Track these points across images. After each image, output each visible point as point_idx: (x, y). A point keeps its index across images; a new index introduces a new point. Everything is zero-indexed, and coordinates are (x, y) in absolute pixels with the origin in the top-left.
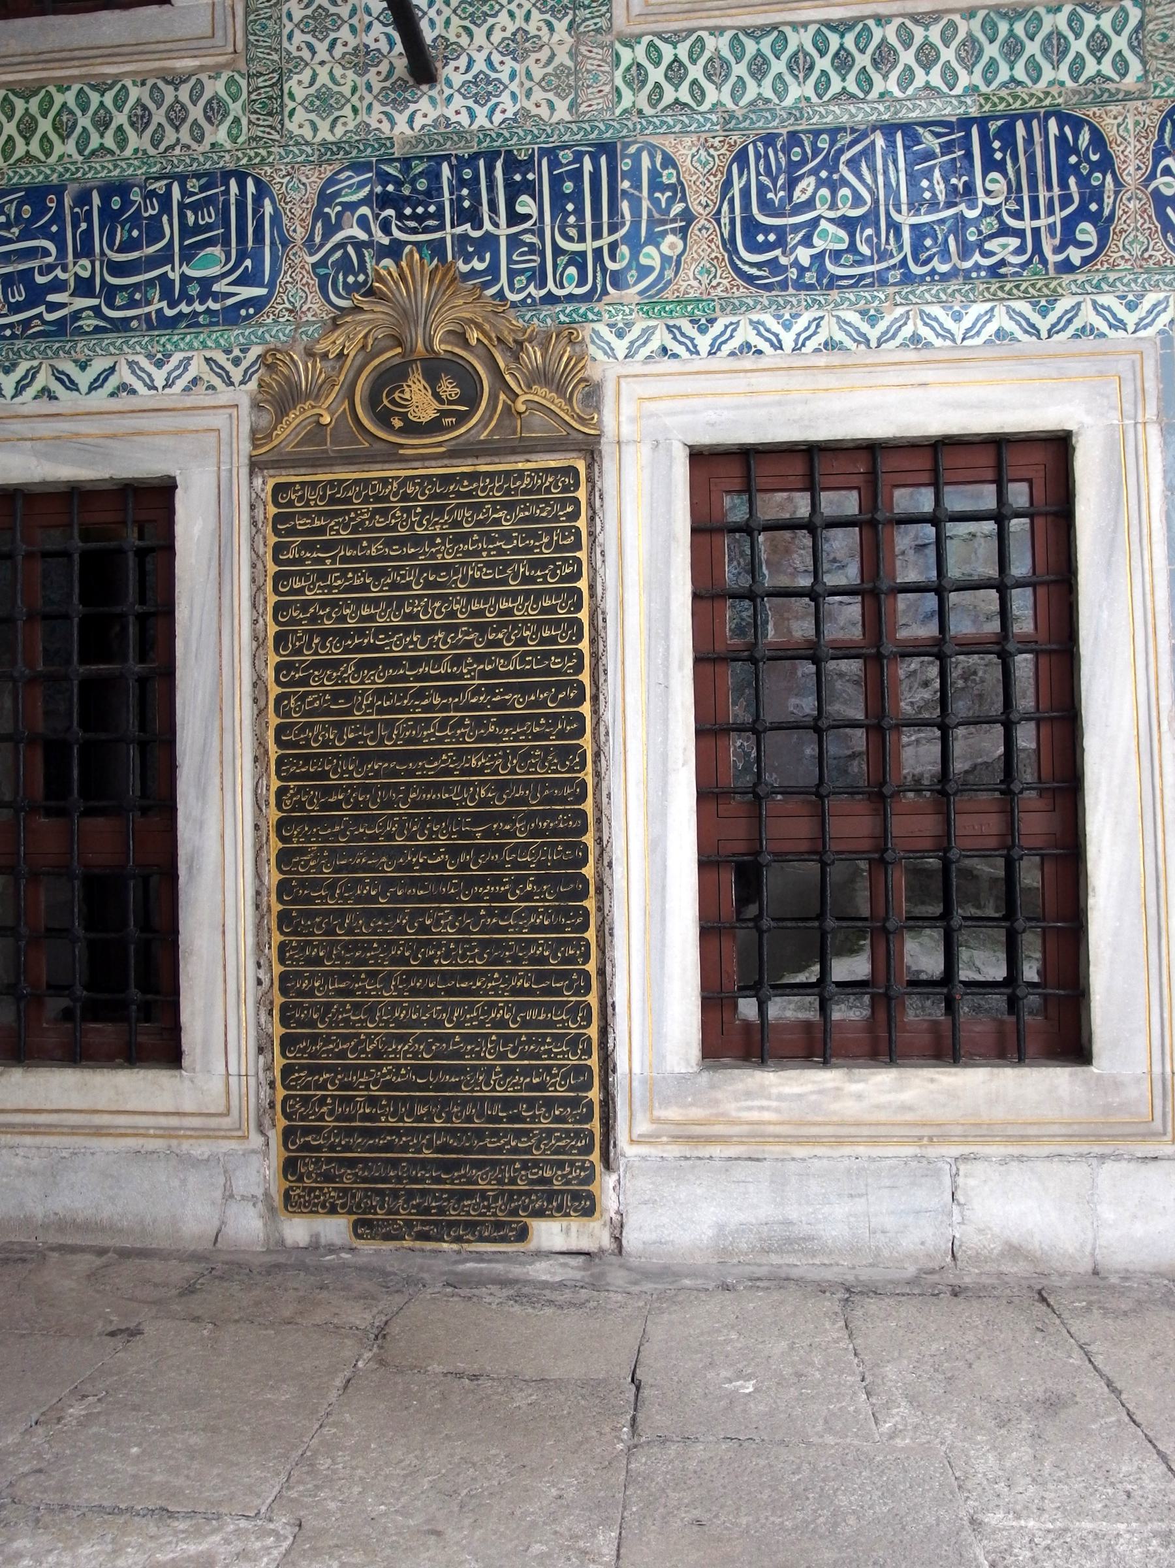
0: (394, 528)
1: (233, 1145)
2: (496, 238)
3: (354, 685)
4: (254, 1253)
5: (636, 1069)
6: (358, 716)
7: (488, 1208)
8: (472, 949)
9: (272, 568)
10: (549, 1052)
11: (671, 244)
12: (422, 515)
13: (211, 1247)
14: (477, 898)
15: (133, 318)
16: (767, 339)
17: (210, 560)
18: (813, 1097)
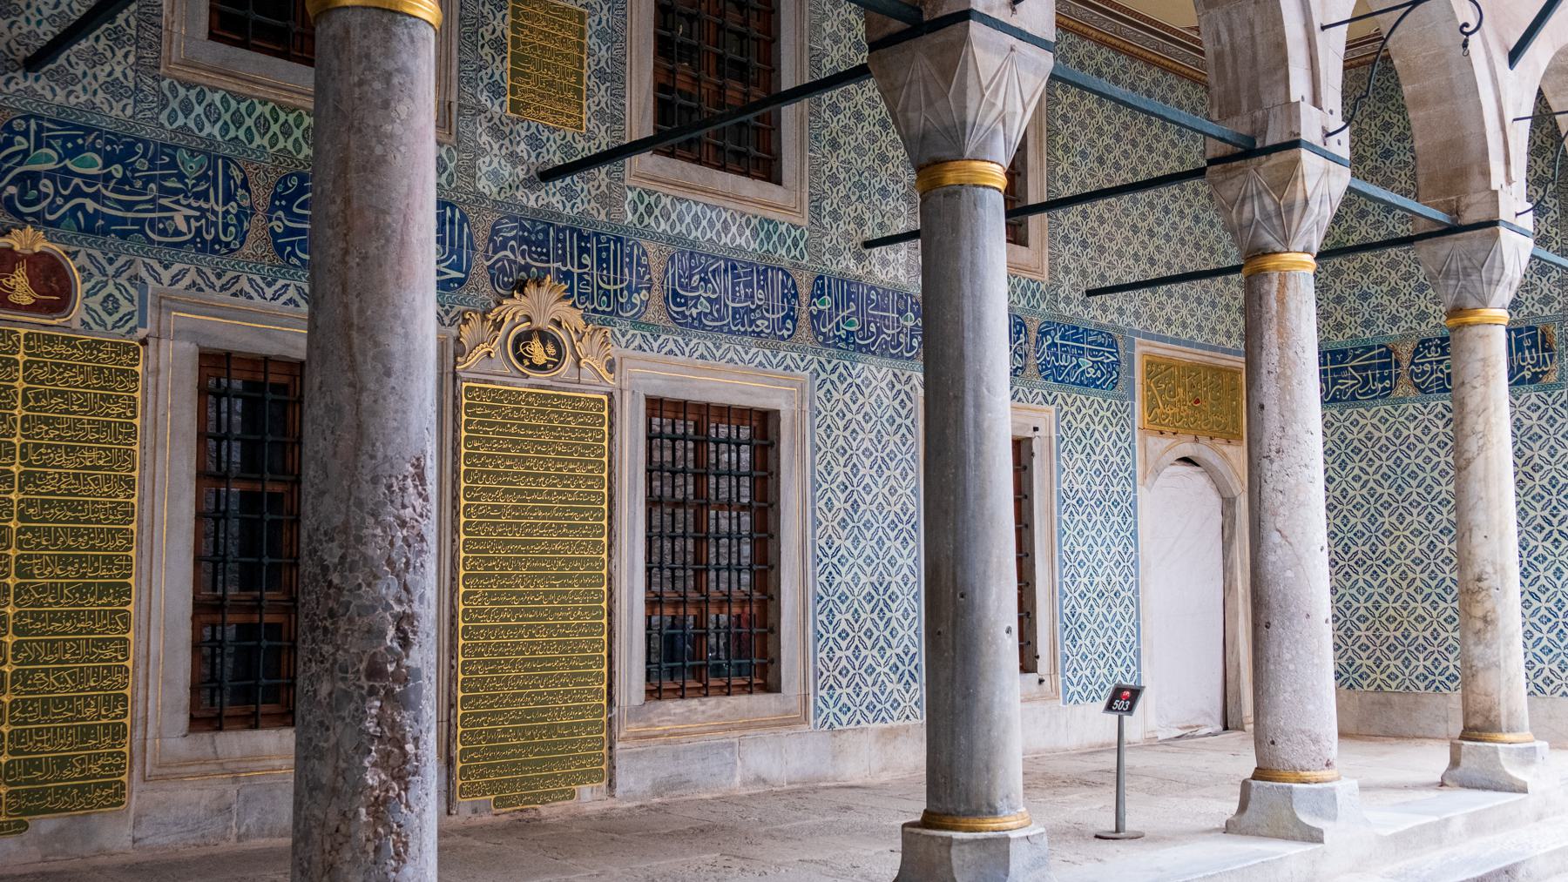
6: (503, 519)
11: (644, 294)
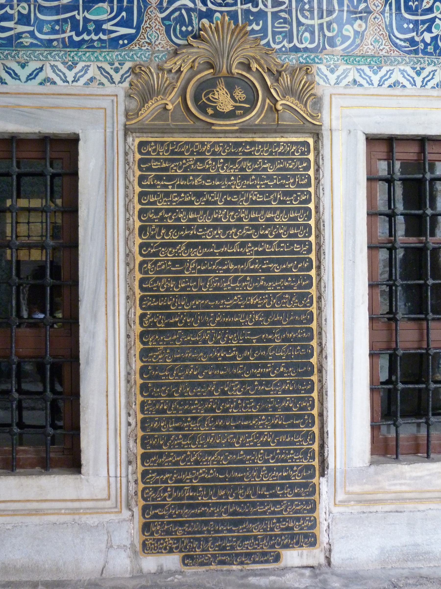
0: (208, 170)
1: (113, 517)
2: (266, 13)
3: (185, 257)
4: (126, 578)
5: (338, 466)
6: (187, 274)
7: (258, 545)
8: (250, 403)
9: (138, 189)
10: (292, 458)
12: (224, 163)
13: (99, 577)
14: (253, 375)
15: (55, 40)
16: (408, 80)
17: (100, 183)
18: (428, 478)
